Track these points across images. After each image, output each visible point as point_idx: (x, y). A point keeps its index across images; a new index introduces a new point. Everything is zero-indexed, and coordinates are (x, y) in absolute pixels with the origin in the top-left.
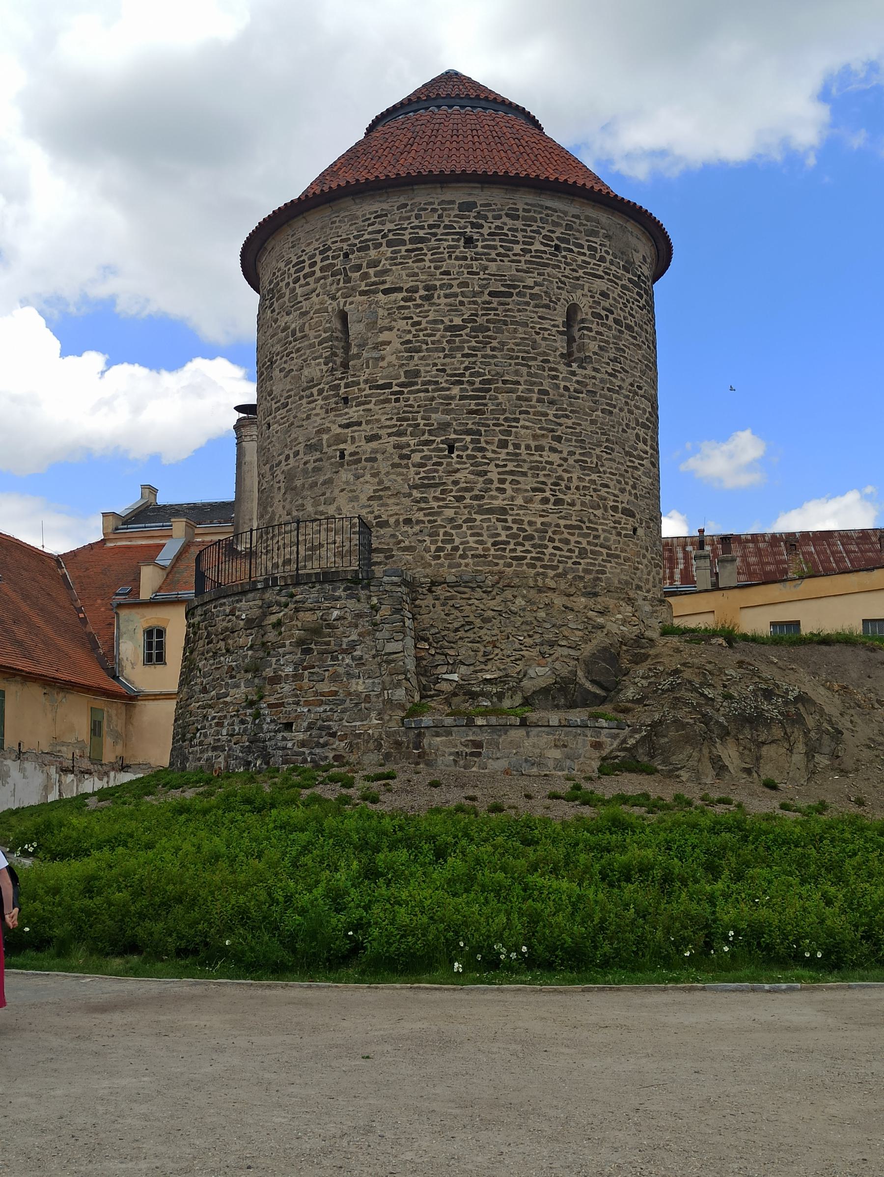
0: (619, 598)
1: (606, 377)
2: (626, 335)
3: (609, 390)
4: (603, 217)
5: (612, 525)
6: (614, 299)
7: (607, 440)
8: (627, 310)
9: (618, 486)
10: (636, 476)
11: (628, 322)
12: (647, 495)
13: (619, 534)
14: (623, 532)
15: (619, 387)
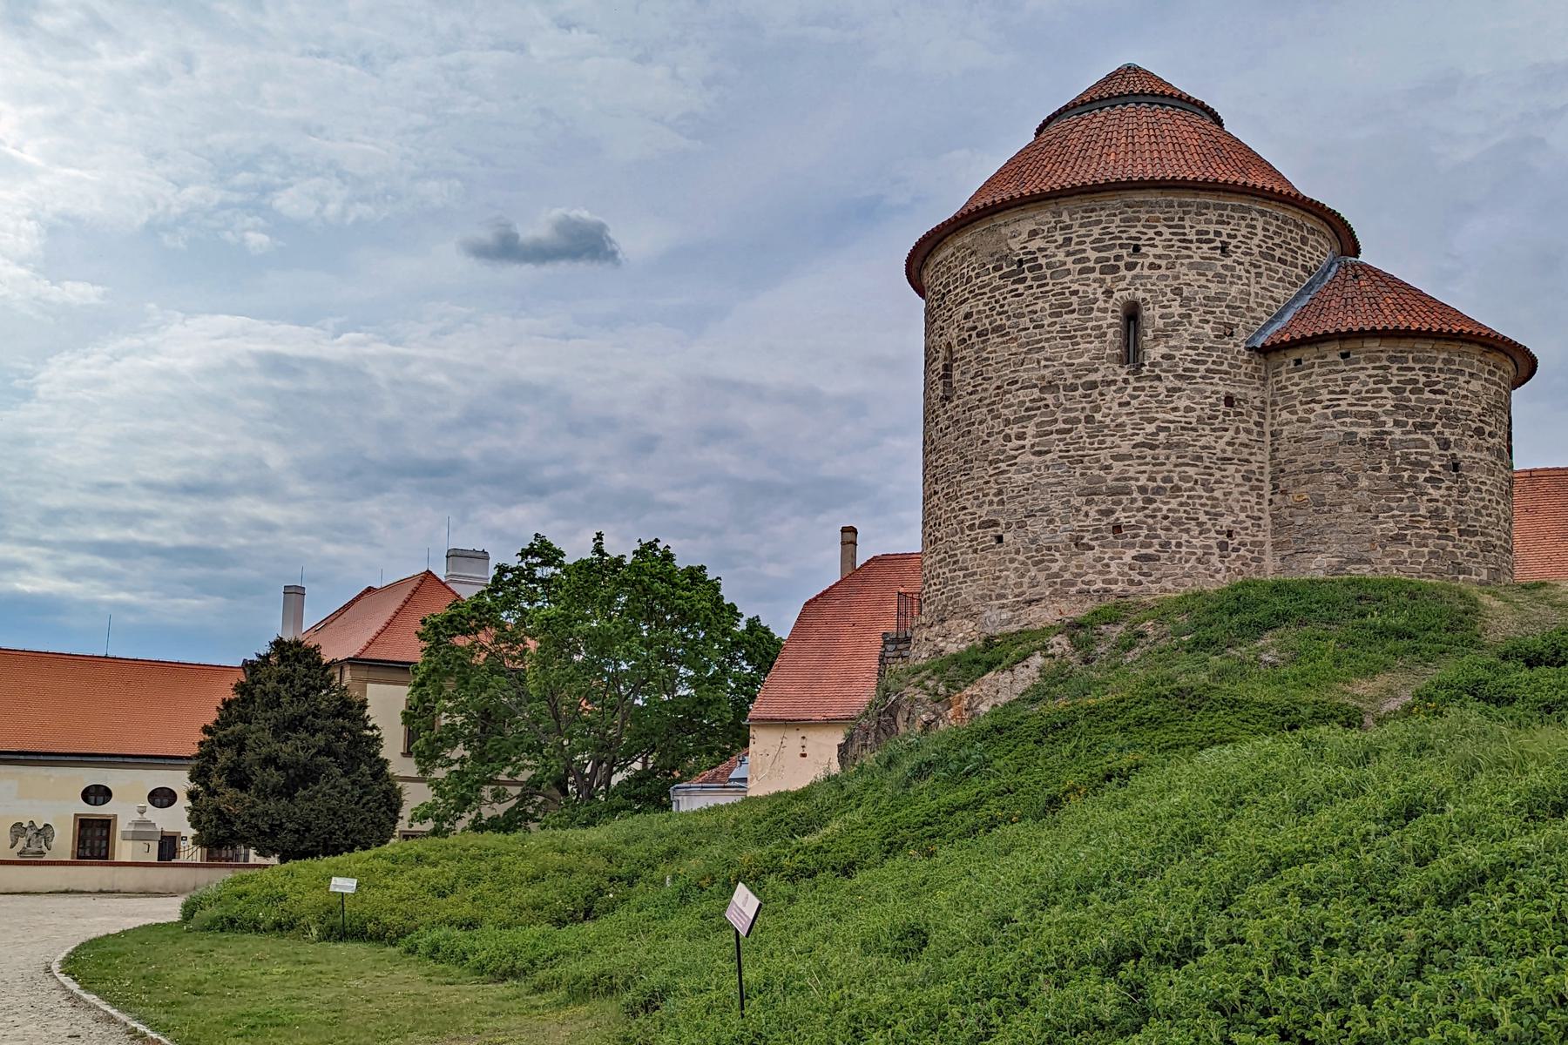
0: (962, 618)
1: (968, 397)
2: (994, 339)
3: (969, 410)
4: (966, 239)
5: (969, 544)
6: (979, 312)
7: (965, 462)
8: (995, 312)
9: (976, 502)
10: (1000, 481)
11: (999, 322)
12: (1023, 492)
13: (975, 551)
14: (980, 547)
15: (980, 401)
